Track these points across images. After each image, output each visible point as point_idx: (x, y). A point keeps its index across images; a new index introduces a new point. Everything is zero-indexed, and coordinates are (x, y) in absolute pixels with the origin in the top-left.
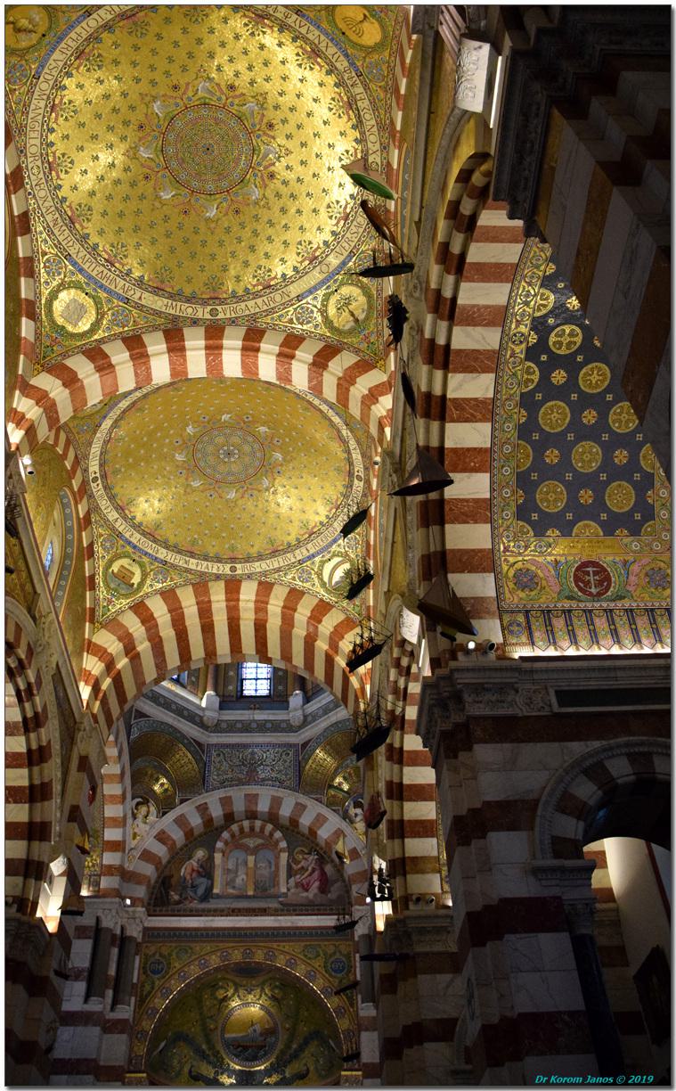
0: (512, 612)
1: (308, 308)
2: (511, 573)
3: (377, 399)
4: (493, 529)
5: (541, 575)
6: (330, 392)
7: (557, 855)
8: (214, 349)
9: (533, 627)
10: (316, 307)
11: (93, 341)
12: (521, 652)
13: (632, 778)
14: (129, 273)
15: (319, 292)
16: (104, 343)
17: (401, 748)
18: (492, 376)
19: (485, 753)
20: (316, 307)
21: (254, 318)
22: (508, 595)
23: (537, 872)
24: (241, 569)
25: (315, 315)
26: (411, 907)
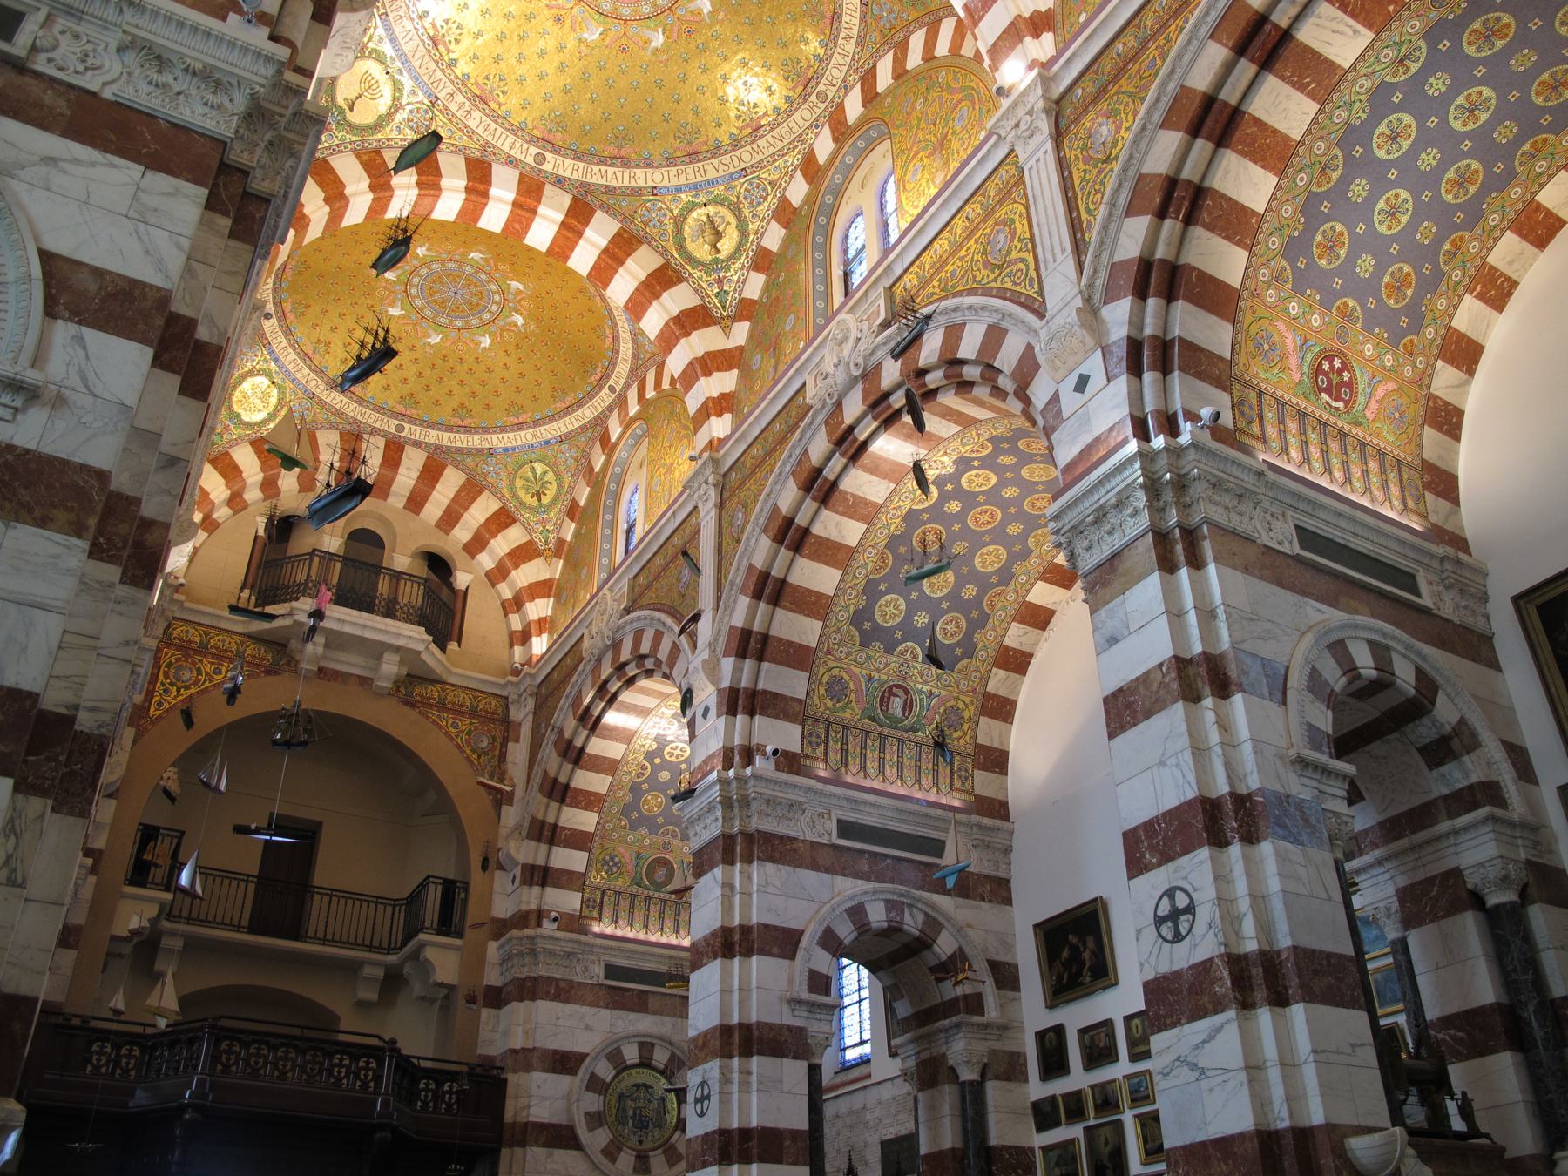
0: (816, 720)
2: (825, 680)
4: (824, 627)
5: (852, 686)
6: (654, 321)
8: (525, 209)
9: (831, 743)
11: (376, 140)
14: (453, 63)
15: (683, 196)
17: (582, 750)
18: (892, 486)
21: (585, 186)
22: (817, 701)
23: (795, 1002)
24: (410, 431)
26: (546, 923)
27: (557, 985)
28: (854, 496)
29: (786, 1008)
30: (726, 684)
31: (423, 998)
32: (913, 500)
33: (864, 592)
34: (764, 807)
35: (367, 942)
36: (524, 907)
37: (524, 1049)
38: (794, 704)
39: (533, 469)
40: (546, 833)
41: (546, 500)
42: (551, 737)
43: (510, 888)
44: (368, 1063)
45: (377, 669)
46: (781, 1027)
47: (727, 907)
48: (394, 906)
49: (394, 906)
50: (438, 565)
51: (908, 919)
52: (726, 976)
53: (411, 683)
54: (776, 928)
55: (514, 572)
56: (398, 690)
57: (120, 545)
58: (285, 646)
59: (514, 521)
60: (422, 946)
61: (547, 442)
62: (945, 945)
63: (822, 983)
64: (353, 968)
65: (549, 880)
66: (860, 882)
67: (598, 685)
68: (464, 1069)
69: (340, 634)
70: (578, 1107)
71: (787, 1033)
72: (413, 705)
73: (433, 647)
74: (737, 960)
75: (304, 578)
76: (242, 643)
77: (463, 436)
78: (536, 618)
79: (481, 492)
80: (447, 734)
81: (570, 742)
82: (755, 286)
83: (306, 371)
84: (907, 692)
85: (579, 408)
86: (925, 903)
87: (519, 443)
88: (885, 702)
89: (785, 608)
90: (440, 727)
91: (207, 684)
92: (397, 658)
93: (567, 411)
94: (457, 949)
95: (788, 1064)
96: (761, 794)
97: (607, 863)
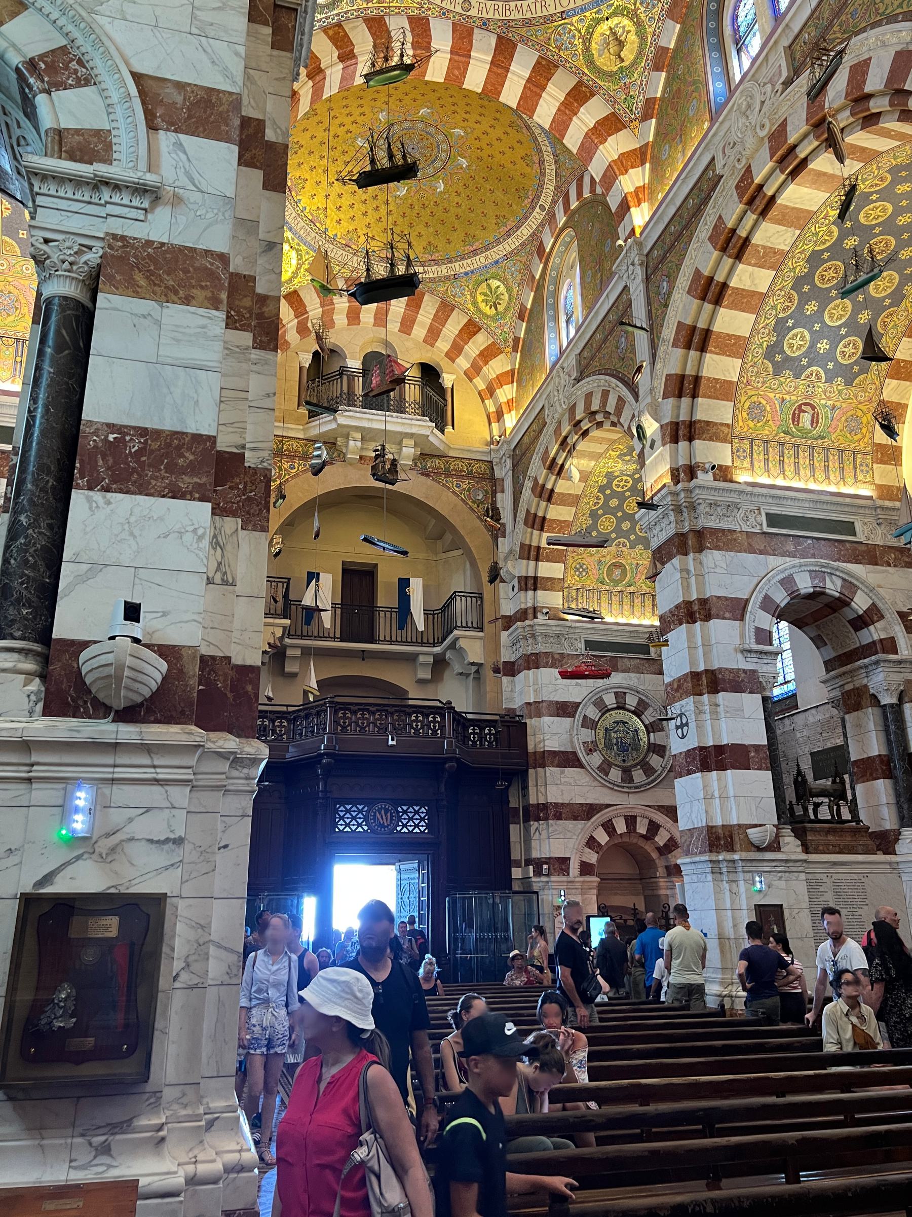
1: (571, 30)
3: (626, 171)
4: (743, 363)
5: (768, 408)
7: (758, 642)
9: (755, 455)
10: (580, 32)
12: (742, 477)
13: (811, 590)
15: (587, 14)
16: (348, 19)
18: (798, 232)
19: (714, 558)
20: (580, 32)
21: (507, 24)
22: (741, 423)
25: (576, 42)
27: (553, 657)
28: (764, 247)
29: (740, 656)
30: (667, 420)
31: (461, 674)
32: (815, 242)
33: (774, 330)
34: (707, 509)
35: (419, 641)
36: (523, 606)
37: (535, 702)
38: (723, 428)
39: (488, 285)
40: (533, 553)
41: (501, 308)
42: (528, 484)
43: (511, 594)
44: (434, 718)
45: (400, 453)
46: (739, 670)
47: (687, 588)
48: (433, 615)
49: (433, 615)
50: (429, 373)
51: (829, 584)
52: (690, 636)
53: (424, 459)
54: (726, 599)
55: (484, 368)
56: (416, 466)
57: (248, 315)
58: (334, 444)
59: (480, 329)
60: (457, 639)
61: (497, 262)
62: (860, 603)
63: (764, 636)
64: (412, 658)
65: (539, 585)
66: (788, 559)
67: (559, 442)
68: (497, 718)
69: (370, 429)
70: (578, 739)
71: (743, 675)
72: (428, 475)
73: (436, 431)
74: (698, 624)
75: (339, 392)
76: (306, 445)
77: (433, 268)
78: (505, 400)
79: (453, 310)
80: (454, 492)
81: (543, 486)
82: (658, 84)
83: (313, 234)
84: (813, 408)
85: (518, 228)
86: (842, 572)
87: (476, 266)
88: (796, 419)
89: (711, 352)
90: (449, 488)
91: (287, 477)
92: (412, 442)
93: (508, 234)
94: (480, 638)
95: (746, 696)
96: (705, 500)
97: (578, 569)
